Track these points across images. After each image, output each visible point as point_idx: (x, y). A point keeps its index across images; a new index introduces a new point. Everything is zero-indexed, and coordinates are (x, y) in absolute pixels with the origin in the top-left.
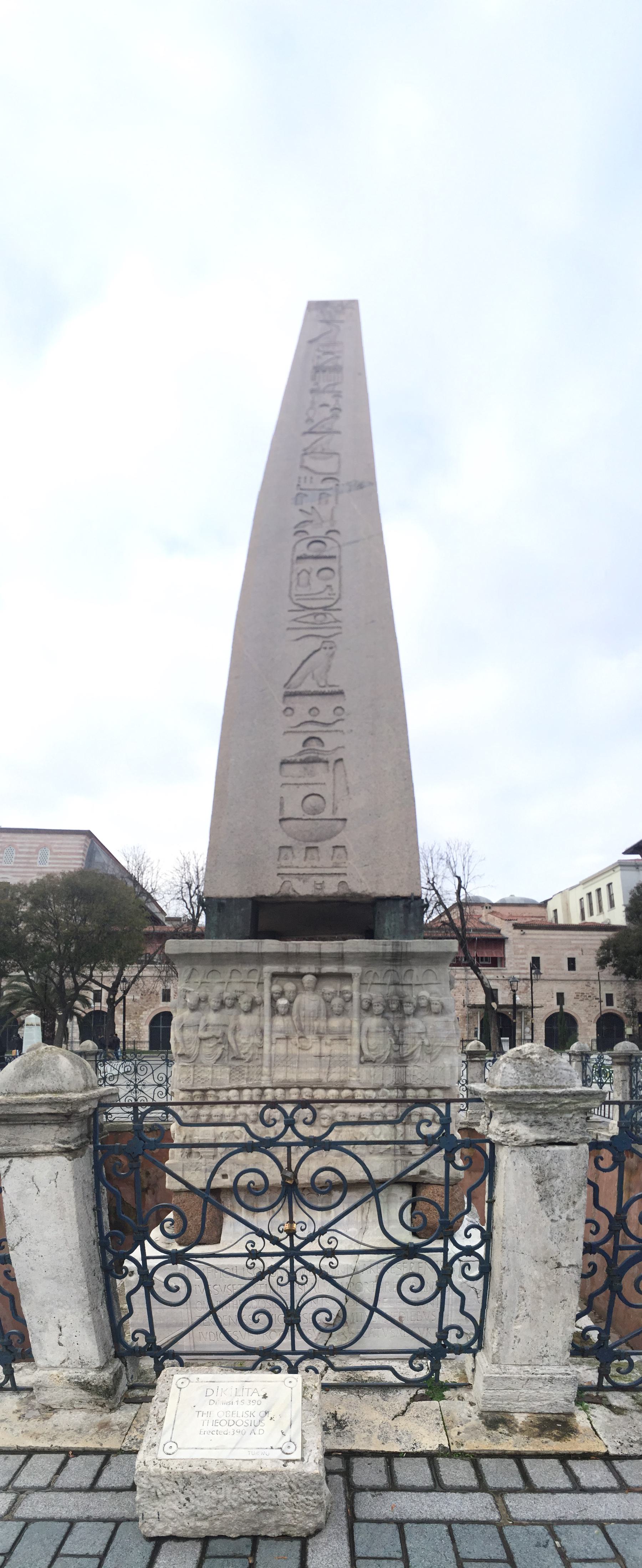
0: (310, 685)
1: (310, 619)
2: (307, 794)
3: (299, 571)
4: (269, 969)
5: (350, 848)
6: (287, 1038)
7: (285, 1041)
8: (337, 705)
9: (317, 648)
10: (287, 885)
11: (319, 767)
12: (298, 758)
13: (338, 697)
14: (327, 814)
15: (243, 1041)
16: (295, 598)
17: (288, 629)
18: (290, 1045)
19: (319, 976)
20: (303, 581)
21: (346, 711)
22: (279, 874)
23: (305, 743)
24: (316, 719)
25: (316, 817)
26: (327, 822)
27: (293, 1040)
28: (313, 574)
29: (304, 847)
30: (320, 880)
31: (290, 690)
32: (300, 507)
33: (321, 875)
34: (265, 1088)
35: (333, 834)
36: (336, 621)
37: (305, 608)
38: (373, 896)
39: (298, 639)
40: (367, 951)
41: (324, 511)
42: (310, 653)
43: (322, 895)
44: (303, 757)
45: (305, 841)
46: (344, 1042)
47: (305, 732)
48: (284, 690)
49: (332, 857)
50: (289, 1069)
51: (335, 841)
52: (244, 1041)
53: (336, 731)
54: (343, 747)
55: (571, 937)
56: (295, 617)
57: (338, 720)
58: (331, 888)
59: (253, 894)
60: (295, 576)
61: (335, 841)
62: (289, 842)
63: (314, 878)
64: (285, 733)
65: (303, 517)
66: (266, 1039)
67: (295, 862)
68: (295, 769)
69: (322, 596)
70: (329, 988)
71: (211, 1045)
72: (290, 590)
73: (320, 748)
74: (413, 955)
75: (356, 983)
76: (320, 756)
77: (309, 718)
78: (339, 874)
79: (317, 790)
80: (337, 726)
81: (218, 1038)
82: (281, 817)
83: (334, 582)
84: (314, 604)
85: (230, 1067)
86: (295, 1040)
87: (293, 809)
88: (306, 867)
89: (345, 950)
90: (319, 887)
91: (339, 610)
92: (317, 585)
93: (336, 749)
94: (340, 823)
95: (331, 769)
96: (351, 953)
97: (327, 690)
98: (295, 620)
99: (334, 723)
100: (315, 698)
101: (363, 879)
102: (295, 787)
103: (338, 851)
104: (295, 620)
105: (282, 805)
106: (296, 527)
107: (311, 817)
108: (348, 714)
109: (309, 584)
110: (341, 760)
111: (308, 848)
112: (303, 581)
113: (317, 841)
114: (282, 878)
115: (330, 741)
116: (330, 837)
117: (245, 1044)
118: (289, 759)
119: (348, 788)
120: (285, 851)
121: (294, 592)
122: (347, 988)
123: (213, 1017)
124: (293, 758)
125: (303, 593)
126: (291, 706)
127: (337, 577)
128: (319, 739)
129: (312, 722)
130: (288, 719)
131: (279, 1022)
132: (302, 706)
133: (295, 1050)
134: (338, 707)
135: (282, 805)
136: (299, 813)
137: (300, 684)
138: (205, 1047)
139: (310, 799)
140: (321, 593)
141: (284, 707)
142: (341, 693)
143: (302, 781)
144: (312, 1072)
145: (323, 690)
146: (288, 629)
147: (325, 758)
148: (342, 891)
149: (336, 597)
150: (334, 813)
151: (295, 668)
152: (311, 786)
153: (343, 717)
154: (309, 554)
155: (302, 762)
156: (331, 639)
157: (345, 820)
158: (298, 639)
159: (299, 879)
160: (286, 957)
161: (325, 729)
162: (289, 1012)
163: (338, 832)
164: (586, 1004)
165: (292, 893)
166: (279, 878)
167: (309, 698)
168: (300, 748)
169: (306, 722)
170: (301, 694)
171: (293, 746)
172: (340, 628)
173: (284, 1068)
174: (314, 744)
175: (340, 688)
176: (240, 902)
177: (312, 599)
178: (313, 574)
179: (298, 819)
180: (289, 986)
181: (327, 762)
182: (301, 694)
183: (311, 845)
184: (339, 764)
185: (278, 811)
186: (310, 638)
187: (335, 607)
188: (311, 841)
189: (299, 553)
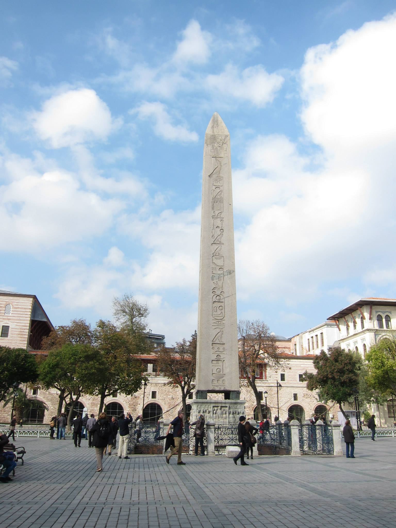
0: (217, 342)
1: (217, 323)
4: (212, 405)
14: (221, 373)
19: (222, 407)
20: (215, 310)
28: (218, 308)
35: (223, 377)
41: (220, 283)
55: (301, 363)
61: (223, 379)
70: (223, 409)
74: (238, 403)
75: (228, 408)
80: (223, 352)
83: (223, 311)
87: (215, 371)
92: (219, 312)
109: (216, 311)
112: (215, 310)
131: (214, 415)
132: (216, 346)
162: (216, 414)
164: (308, 400)
171: (214, 357)
174: (218, 357)
178: (218, 308)
180: (216, 408)
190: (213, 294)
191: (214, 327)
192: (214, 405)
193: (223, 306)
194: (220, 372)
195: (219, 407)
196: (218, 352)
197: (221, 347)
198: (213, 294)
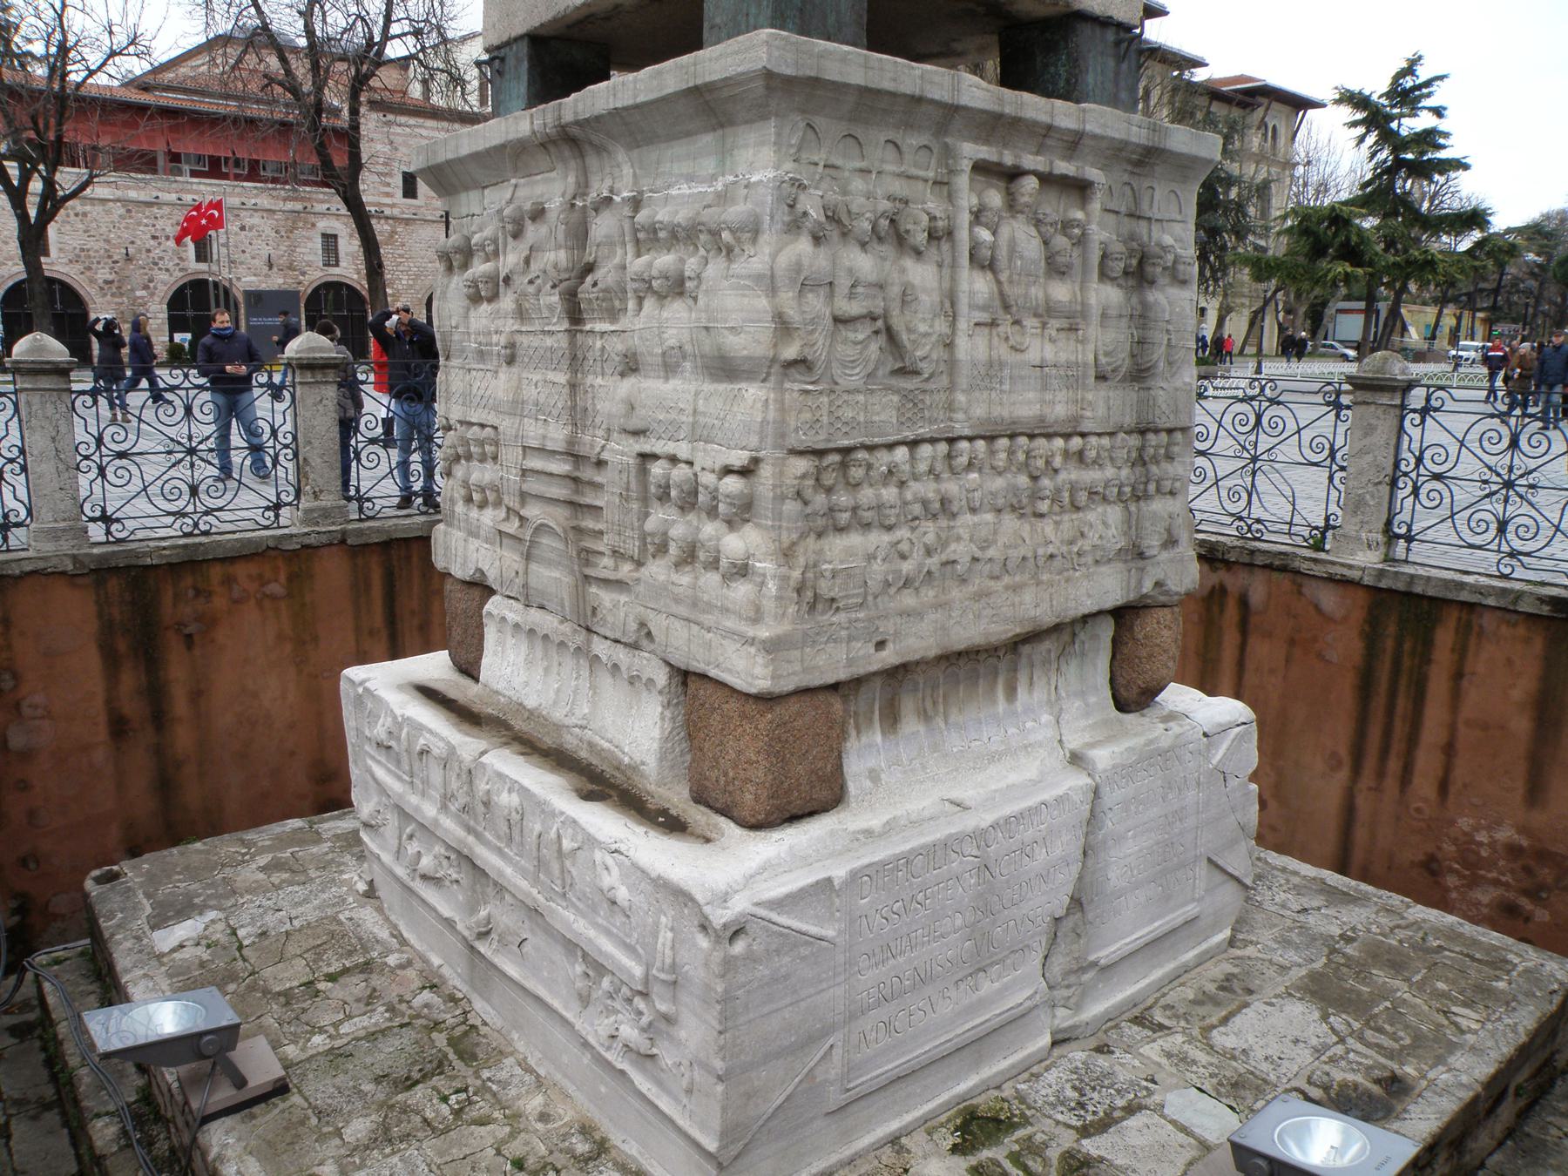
6: (993, 324)
7: (986, 330)
15: (923, 328)
18: (995, 340)
19: (1046, 179)
27: (1001, 329)
34: (951, 441)
46: (1073, 336)
50: (994, 394)
52: (921, 328)
66: (962, 324)
71: (861, 337)
81: (874, 319)
85: (898, 392)
86: (1006, 328)
89: (1088, 128)
96: (1095, 137)
117: (926, 335)
122: (1079, 215)
123: (864, 263)
133: (1003, 351)
138: (845, 341)
144: (1029, 402)
160: (994, 125)
173: (986, 394)
192: (985, 152)
195: (1031, 183)
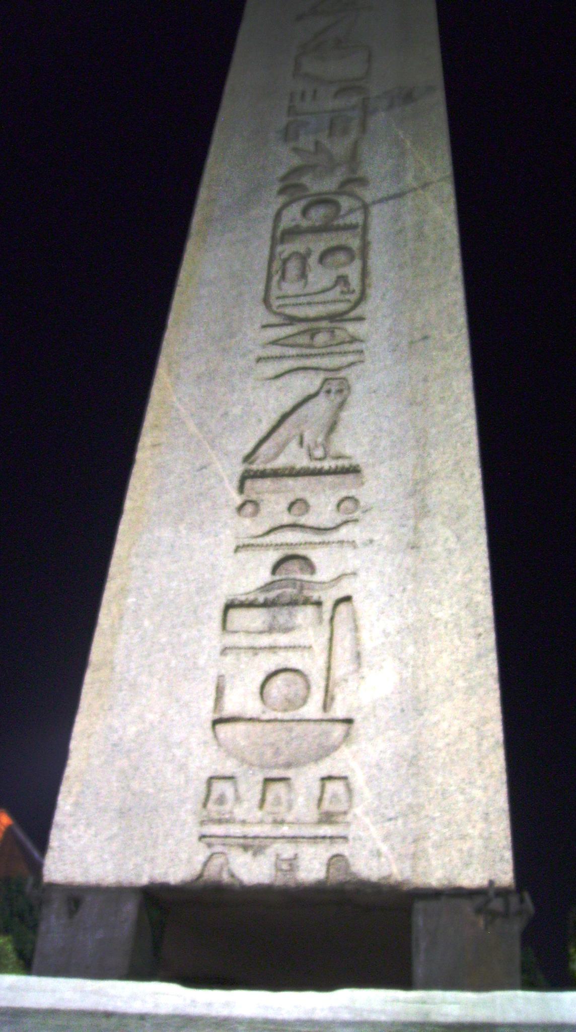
0: (294, 456)
1: (304, 339)
2: (273, 668)
3: (285, 255)
5: (359, 780)
8: (344, 494)
9: (312, 390)
10: (217, 861)
11: (304, 615)
12: (261, 598)
13: (349, 478)
14: (312, 709)
16: (275, 303)
17: (259, 360)
21: (362, 504)
22: (202, 837)
23: (275, 569)
24: (303, 520)
25: (287, 716)
26: (312, 726)
29: (260, 777)
30: (288, 850)
31: (255, 467)
32: (293, 144)
33: (294, 839)
35: (325, 751)
36: (353, 340)
37: (292, 320)
38: (405, 888)
39: (277, 377)
40: (383, 1018)
42: (299, 399)
43: (292, 884)
44: (272, 595)
45: (262, 767)
47: (277, 546)
48: (240, 469)
49: (320, 800)
51: (326, 767)
53: (341, 542)
54: (354, 574)
56: (275, 338)
57: (346, 522)
58: (312, 868)
59: (144, 880)
60: (277, 265)
61: (326, 767)
62: (229, 766)
63: (278, 846)
64: (237, 549)
65: (296, 161)
67: (240, 812)
68: (256, 618)
69: (330, 296)
72: (267, 289)
73: (306, 577)
76: (306, 593)
77: (287, 519)
78: (331, 838)
79: (294, 660)
80: (343, 533)
82: (217, 716)
84: (312, 312)
87: (242, 698)
88: (261, 822)
90: (285, 866)
91: (360, 319)
93: (339, 579)
94: (338, 730)
95: (327, 616)
97: (326, 465)
98: (275, 343)
99: (336, 528)
100: (302, 481)
101: (384, 848)
102: (250, 653)
103: (331, 787)
104: (275, 343)
105: (220, 691)
106: (284, 178)
107: (280, 715)
108: (365, 512)
110: (347, 599)
111: (268, 781)
113: (288, 765)
114: (209, 845)
115: (326, 562)
116: (318, 759)
118: (243, 598)
119: (358, 656)
120: (220, 787)
121: (275, 292)
124: (251, 597)
125: (290, 293)
126: (254, 497)
127: (357, 263)
128: (304, 559)
129: (293, 526)
130: (247, 522)
132: (275, 502)
134: (347, 498)
135: (220, 691)
136: (253, 707)
137: (276, 455)
139: (279, 681)
140: (324, 291)
141: (238, 500)
142: (354, 470)
143: (265, 640)
145: (318, 465)
146: (259, 360)
147: (315, 596)
148: (337, 877)
149: (353, 298)
150: (325, 707)
151: (265, 427)
152: (282, 653)
153: (356, 515)
154: (305, 223)
155: (266, 604)
156: (342, 374)
157: (349, 721)
158: (277, 377)
159: (246, 848)
161: (316, 538)
163: (335, 748)
165: (225, 878)
166: (202, 846)
167: (290, 482)
168: (264, 576)
169: (282, 527)
170: (276, 474)
172: (361, 352)
174: (294, 571)
175: (354, 462)
176: (113, 895)
177: (309, 304)
178: (313, 260)
179: (251, 720)
181: (319, 604)
182: (276, 474)
183: (275, 773)
184: (343, 607)
185: (210, 703)
186: (301, 374)
187: (352, 314)
188: (277, 766)
189: (286, 222)
190: (282, 200)
191: (271, 369)
193: (355, 243)
194: (291, 703)
196: (290, 537)
197: (323, 503)
198: (282, 200)
